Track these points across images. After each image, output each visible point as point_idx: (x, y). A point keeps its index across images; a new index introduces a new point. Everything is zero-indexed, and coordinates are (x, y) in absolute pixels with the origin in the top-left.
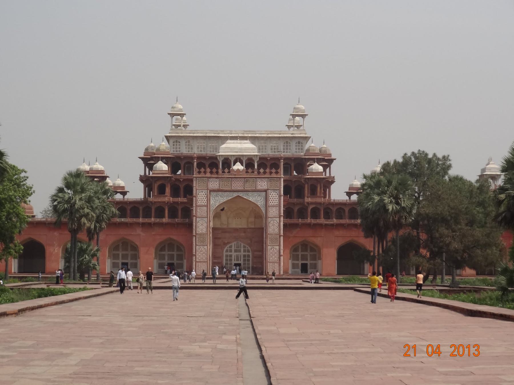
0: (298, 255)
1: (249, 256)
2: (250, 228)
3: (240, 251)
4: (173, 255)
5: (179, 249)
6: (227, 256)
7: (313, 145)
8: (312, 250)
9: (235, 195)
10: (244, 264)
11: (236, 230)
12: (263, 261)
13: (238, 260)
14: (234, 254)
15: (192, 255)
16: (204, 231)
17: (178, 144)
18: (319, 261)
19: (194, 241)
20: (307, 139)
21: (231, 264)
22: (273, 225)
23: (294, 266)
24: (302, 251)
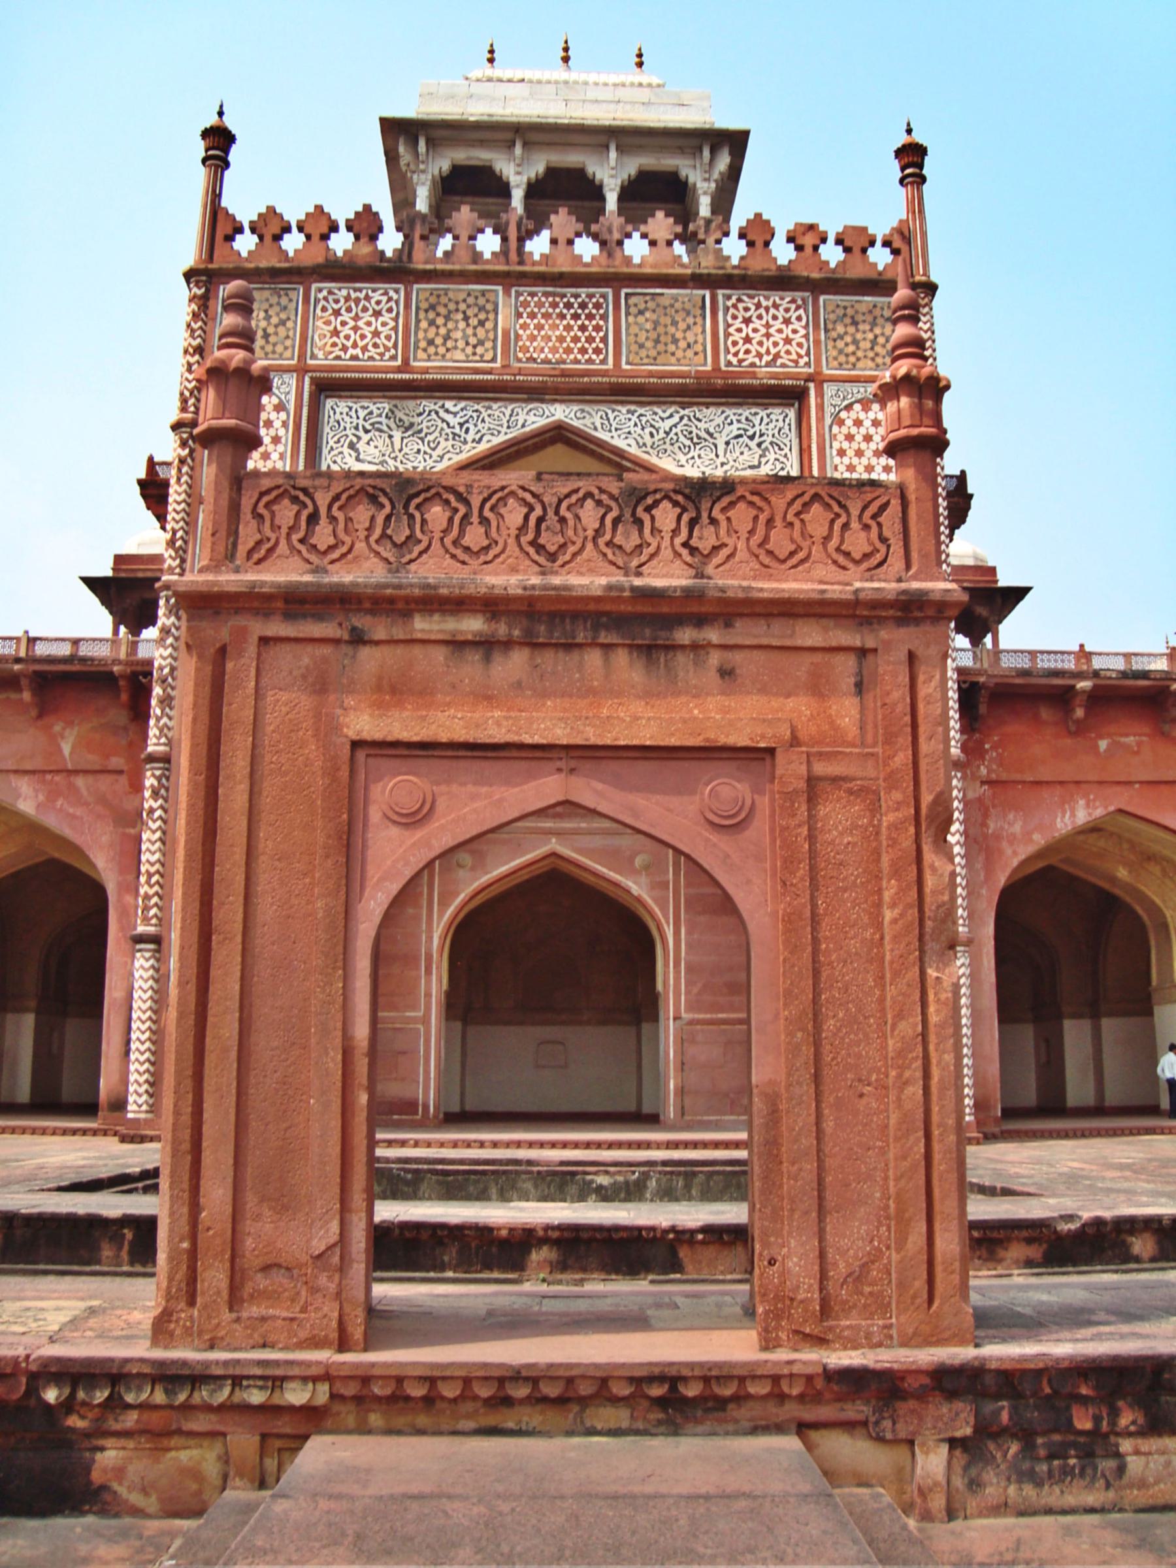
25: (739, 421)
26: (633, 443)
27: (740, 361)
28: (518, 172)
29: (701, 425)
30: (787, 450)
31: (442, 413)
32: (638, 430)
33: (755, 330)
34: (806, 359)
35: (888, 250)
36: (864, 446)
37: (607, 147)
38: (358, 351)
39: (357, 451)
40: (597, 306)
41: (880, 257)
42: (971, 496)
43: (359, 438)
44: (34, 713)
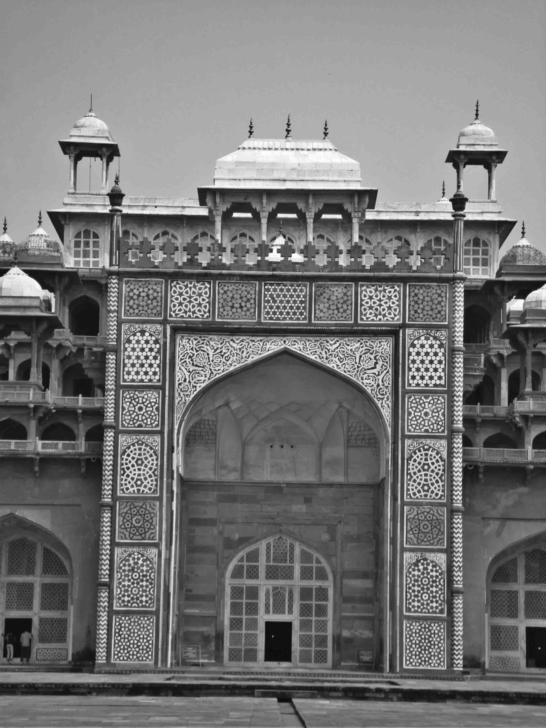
0: (514, 595)
2: (331, 485)
3: (288, 574)
4: (30, 586)
5: (53, 564)
6: (237, 592)
7: (524, 242)
9: (274, 346)
10: (305, 625)
11: (275, 489)
12: (381, 611)
13: (279, 609)
14: (264, 585)
15: (95, 585)
16: (148, 486)
17: (91, 240)
19: (106, 529)
20: (503, 228)
21: (253, 624)
23: (500, 638)
24: (528, 581)
25: (366, 346)
26: (317, 356)
27: (367, 318)
29: (349, 348)
30: (388, 360)
31: (231, 343)
32: (320, 351)
33: (374, 303)
34: (398, 317)
36: (425, 358)
38: (191, 314)
39: (192, 360)
40: (301, 291)
43: (194, 355)
44: (38, 474)
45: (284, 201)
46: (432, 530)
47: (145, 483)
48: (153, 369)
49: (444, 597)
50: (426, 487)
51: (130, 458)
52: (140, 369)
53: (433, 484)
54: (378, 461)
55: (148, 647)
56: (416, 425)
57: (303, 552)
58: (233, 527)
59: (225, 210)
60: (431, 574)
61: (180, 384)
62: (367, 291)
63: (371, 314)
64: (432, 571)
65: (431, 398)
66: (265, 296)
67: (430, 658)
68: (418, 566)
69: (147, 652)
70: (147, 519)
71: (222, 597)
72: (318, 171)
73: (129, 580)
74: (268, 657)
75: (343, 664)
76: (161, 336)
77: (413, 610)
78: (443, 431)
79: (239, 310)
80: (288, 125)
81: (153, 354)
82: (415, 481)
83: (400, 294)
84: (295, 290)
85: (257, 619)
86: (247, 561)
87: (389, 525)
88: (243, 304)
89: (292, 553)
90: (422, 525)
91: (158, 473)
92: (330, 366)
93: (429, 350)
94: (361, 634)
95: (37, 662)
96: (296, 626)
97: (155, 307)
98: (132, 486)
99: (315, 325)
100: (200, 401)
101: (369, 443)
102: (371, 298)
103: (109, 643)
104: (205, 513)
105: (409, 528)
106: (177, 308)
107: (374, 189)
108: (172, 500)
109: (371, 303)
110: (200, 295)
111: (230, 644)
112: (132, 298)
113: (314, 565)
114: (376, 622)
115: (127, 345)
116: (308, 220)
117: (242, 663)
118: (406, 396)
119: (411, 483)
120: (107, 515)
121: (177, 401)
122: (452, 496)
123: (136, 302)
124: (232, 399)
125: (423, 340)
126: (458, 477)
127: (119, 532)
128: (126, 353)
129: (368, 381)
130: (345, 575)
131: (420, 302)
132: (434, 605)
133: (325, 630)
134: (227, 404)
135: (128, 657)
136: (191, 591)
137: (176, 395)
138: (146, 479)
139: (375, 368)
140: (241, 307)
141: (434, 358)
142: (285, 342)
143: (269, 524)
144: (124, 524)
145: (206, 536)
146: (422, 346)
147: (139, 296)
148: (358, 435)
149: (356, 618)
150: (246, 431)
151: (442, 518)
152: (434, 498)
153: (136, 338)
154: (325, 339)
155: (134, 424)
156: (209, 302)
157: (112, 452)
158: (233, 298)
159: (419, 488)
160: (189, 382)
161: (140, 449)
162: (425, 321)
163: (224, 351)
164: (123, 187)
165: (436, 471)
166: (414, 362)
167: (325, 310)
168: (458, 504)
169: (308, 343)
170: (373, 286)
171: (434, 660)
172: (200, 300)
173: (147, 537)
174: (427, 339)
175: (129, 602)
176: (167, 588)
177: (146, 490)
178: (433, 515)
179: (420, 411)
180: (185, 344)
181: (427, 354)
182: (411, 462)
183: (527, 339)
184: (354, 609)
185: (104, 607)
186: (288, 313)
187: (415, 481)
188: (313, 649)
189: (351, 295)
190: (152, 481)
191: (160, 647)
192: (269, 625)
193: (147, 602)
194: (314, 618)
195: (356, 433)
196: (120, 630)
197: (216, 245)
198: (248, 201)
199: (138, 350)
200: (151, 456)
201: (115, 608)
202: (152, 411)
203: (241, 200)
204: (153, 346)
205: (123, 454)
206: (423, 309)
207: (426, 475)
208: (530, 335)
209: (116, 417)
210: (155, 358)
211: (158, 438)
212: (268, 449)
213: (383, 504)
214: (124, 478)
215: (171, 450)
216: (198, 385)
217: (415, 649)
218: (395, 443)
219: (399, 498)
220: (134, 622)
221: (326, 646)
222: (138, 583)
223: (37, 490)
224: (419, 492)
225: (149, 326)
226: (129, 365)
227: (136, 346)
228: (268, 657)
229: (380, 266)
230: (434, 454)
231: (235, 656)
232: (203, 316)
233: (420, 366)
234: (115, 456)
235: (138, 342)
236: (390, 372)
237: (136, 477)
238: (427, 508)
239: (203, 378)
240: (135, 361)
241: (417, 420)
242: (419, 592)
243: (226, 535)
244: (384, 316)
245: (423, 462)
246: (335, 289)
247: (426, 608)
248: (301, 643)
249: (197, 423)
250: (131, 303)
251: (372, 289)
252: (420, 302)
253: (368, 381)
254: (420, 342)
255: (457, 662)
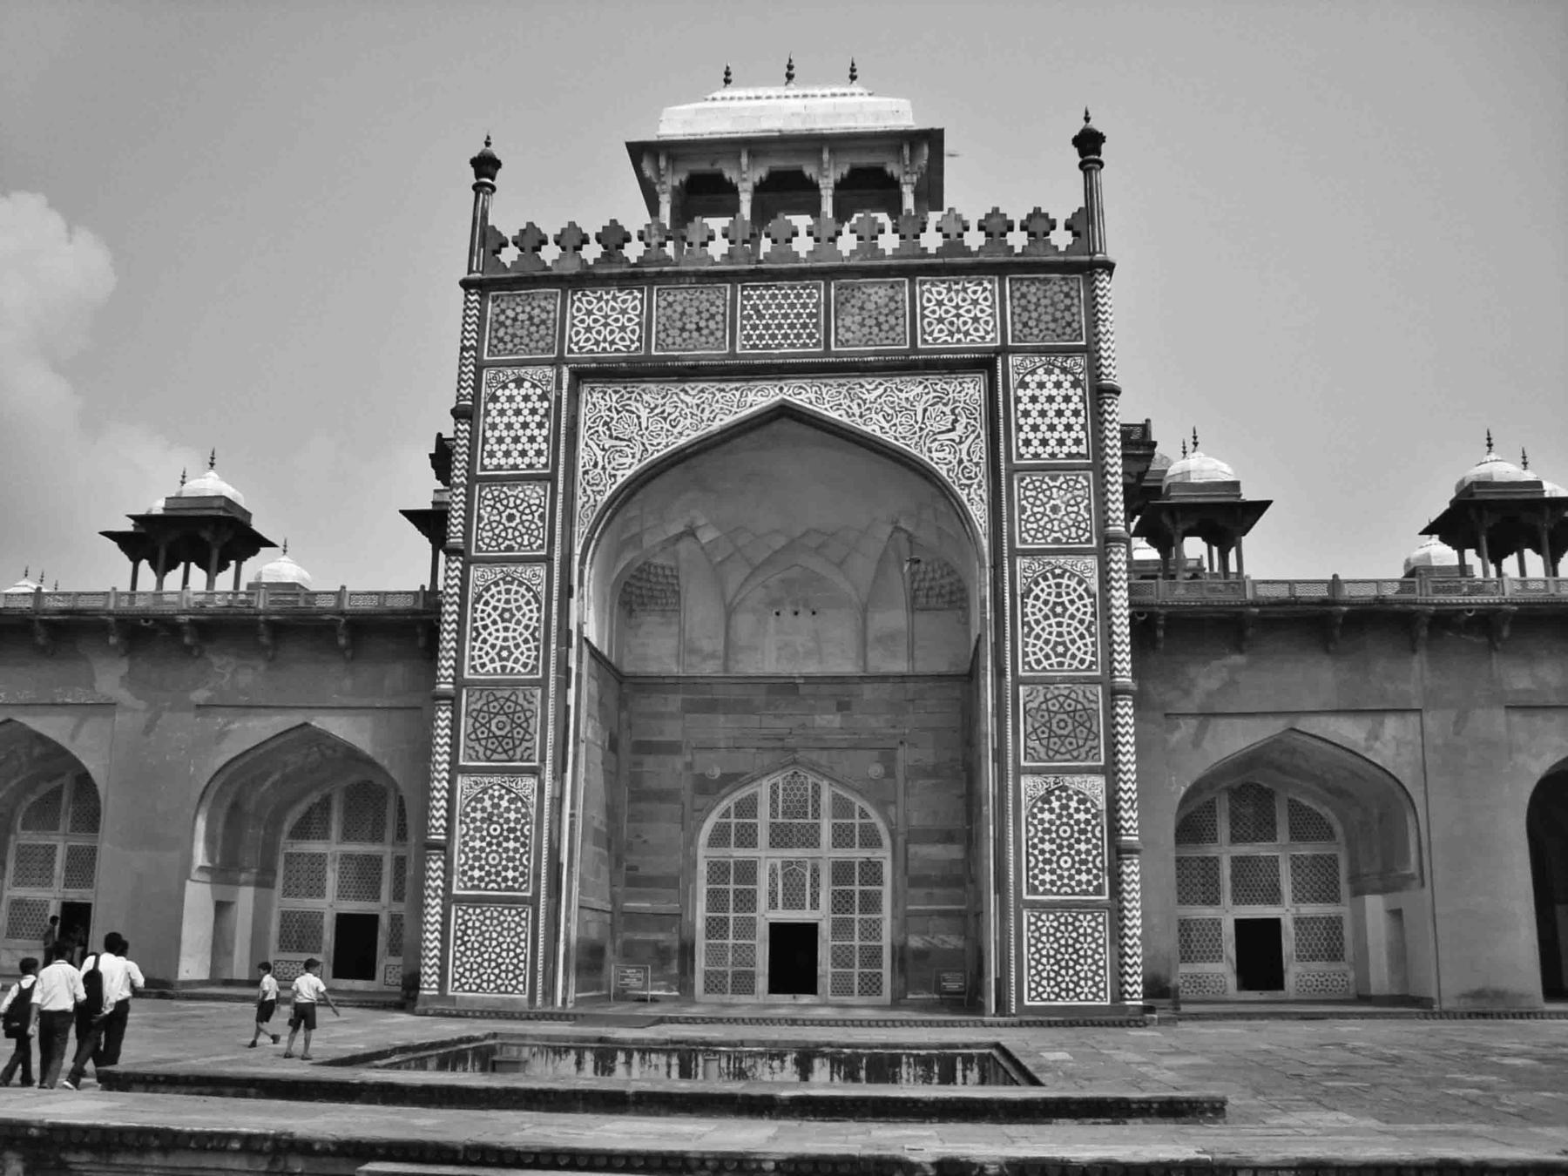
0: (1212, 864)
1: (871, 872)
2: (884, 678)
4: (376, 861)
6: (718, 871)
8: (1306, 826)
9: (760, 397)
10: (842, 928)
11: (784, 688)
12: (979, 898)
13: (793, 902)
14: (767, 858)
18: (1375, 904)
19: (442, 740)
21: (747, 928)
22: (1057, 610)
23: (1193, 940)
27: (935, 339)
28: (746, 178)
29: (903, 395)
31: (682, 395)
32: (847, 401)
33: (947, 312)
35: (1069, 233)
36: (1046, 406)
37: (821, 151)
40: (810, 296)
41: (1061, 238)
42: (1155, 444)
44: (349, 654)
45: (780, 163)
46: (1073, 732)
47: (517, 653)
48: (536, 446)
49: (1102, 862)
50: (1061, 648)
51: (489, 609)
52: (512, 447)
53: (1073, 642)
54: (966, 623)
55: (516, 967)
56: (1037, 531)
57: (836, 798)
58: (712, 755)
59: (677, 183)
60: (1076, 816)
61: (586, 472)
62: (933, 293)
63: (941, 331)
64: (1077, 810)
65: (1062, 479)
66: (744, 307)
67: (1077, 984)
68: (1050, 802)
69: (516, 977)
70: (518, 722)
71: (693, 880)
72: (839, 115)
73: (482, 839)
74: (774, 988)
75: (910, 996)
76: (551, 387)
77: (1041, 889)
78: (1089, 541)
79: (695, 334)
80: (790, 67)
81: (537, 418)
82: (1038, 637)
83: (993, 295)
84: (798, 296)
85: (754, 919)
86: (737, 816)
87: (989, 725)
88: (702, 324)
89: (816, 801)
90: (1054, 722)
91: (540, 634)
92: (868, 429)
93: (1054, 392)
94: (944, 942)
95: (386, 988)
96: (825, 930)
97: (542, 338)
98: (492, 661)
99: (837, 355)
100: (632, 510)
101: (950, 602)
102: (940, 303)
103: (443, 958)
104: (661, 733)
105: (1030, 729)
106: (582, 337)
107: (937, 127)
108: (568, 686)
109: (940, 312)
110: (624, 312)
111: (707, 964)
112: (502, 324)
113: (857, 821)
114: (971, 920)
115: (490, 406)
116: (823, 192)
117: (728, 998)
118: (1016, 477)
119: (1031, 641)
120: (444, 715)
121: (579, 503)
122: (1111, 663)
123: (510, 331)
124: (700, 522)
125: (1041, 375)
126: (1122, 629)
127: (466, 746)
128: (489, 420)
129: (941, 455)
130: (915, 836)
131: (1032, 307)
132: (1084, 877)
133: (879, 937)
134: (691, 532)
135: (479, 986)
136: (635, 868)
137: (579, 492)
138: (517, 646)
139: (953, 429)
140: (699, 329)
141: (1063, 406)
142: (781, 389)
143: (774, 749)
144: (475, 731)
145: (665, 772)
146: (1041, 385)
147: (515, 319)
148: (931, 588)
149: (931, 914)
150: (731, 588)
151: (1094, 706)
152: (1077, 669)
153: (507, 392)
154: (857, 380)
155: (498, 545)
156: (639, 324)
157: (456, 598)
158: (683, 313)
159: (1047, 649)
160: (604, 468)
161: (508, 591)
162: (1043, 340)
163: (668, 410)
164: (497, 151)
165: (1079, 615)
166: (1026, 414)
167: (853, 328)
168: (1125, 677)
169: (824, 390)
170: (943, 282)
171: (1086, 988)
172: (623, 320)
173: (518, 756)
174: (1049, 372)
175: (481, 879)
176: (554, 853)
177: (518, 667)
178: (1077, 701)
179: (1043, 504)
180: (596, 402)
181: (1051, 399)
182: (1030, 601)
183: (1175, 522)
184: (930, 898)
185: (435, 890)
186: (786, 336)
187: (1038, 637)
188: (857, 970)
189: (903, 301)
190: (529, 649)
191: (540, 967)
192: (777, 929)
193: (515, 880)
194: (857, 916)
195: (927, 584)
196: (464, 933)
197: (653, 228)
198: (717, 167)
199: (510, 413)
200: (528, 603)
201: (455, 891)
202: (532, 522)
203: (703, 167)
204: (538, 405)
205: (477, 601)
206: (1038, 320)
207: (1059, 624)
208: (1178, 516)
209: (467, 535)
210: (540, 426)
211: (541, 571)
212: (772, 619)
213: (978, 709)
214: (478, 644)
215: (567, 592)
216: (619, 473)
217: (1047, 966)
218: (997, 566)
219: (1009, 670)
220: (492, 918)
221: (880, 966)
222: (499, 844)
223: (348, 683)
224: (1047, 657)
225: (530, 370)
226: (492, 441)
227: (506, 406)
228: (774, 988)
229: (953, 244)
230: (1073, 584)
231: (714, 983)
232: (628, 347)
233: (1039, 421)
234: (462, 605)
235: (510, 399)
236: (983, 437)
237: (499, 643)
238: (1063, 689)
239: (628, 461)
240: (505, 433)
241: (1037, 521)
242: (1052, 852)
243: (697, 771)
244: (967, 334)
245: (1052, 599)
246: (872, 291)
247: (1068, 885)
248: (834, 959)
249: (640, 570)
250: (501, 333)
251: (942, 288)
252: (1032, 307)
253: (941, 455)
254: (1037, 378)
255: (1131, 990)
